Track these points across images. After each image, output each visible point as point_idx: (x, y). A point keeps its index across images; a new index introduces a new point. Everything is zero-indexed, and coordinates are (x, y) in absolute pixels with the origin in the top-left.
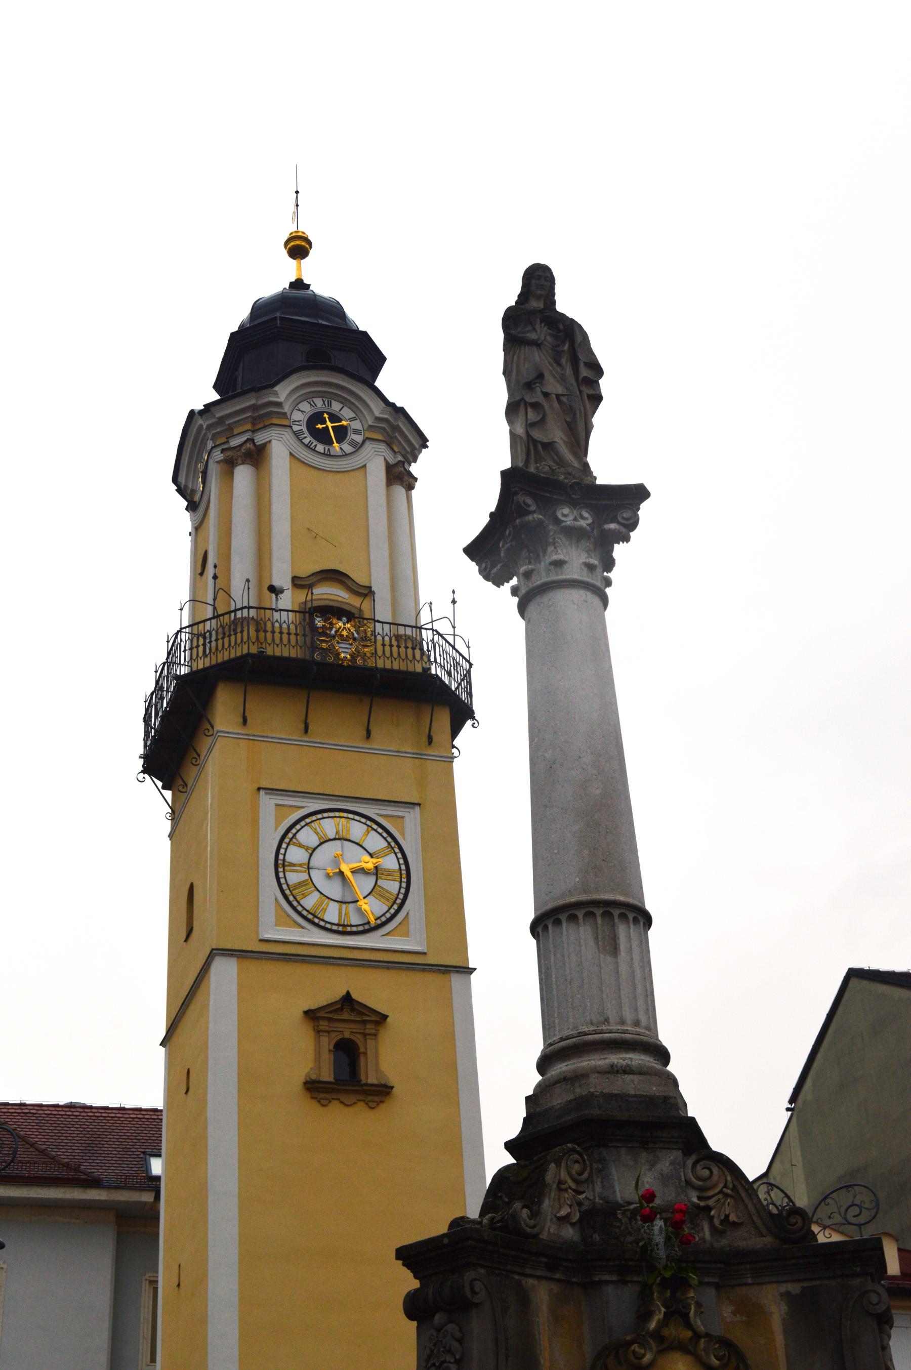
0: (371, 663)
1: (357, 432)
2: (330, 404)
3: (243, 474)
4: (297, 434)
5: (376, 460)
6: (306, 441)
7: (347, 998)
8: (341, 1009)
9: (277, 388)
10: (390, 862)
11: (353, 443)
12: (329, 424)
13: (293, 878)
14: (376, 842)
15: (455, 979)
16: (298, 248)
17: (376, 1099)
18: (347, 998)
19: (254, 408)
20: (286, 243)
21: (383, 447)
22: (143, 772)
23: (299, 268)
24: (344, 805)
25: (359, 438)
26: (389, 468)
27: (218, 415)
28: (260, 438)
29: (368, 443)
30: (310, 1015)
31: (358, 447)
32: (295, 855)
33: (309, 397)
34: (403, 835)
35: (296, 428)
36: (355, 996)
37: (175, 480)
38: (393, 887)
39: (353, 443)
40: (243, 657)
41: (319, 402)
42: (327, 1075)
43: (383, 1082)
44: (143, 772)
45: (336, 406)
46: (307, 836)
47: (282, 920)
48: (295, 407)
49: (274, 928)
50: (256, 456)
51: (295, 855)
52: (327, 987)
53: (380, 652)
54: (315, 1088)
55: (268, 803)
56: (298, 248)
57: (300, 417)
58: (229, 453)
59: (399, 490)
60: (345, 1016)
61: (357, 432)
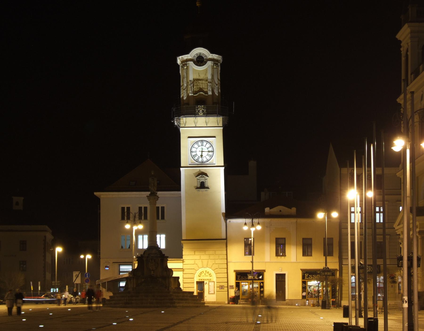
13: (193, 154)
32: (194, 150)
42: (199, 186)
51: (194, 150)
54: (197, 188)
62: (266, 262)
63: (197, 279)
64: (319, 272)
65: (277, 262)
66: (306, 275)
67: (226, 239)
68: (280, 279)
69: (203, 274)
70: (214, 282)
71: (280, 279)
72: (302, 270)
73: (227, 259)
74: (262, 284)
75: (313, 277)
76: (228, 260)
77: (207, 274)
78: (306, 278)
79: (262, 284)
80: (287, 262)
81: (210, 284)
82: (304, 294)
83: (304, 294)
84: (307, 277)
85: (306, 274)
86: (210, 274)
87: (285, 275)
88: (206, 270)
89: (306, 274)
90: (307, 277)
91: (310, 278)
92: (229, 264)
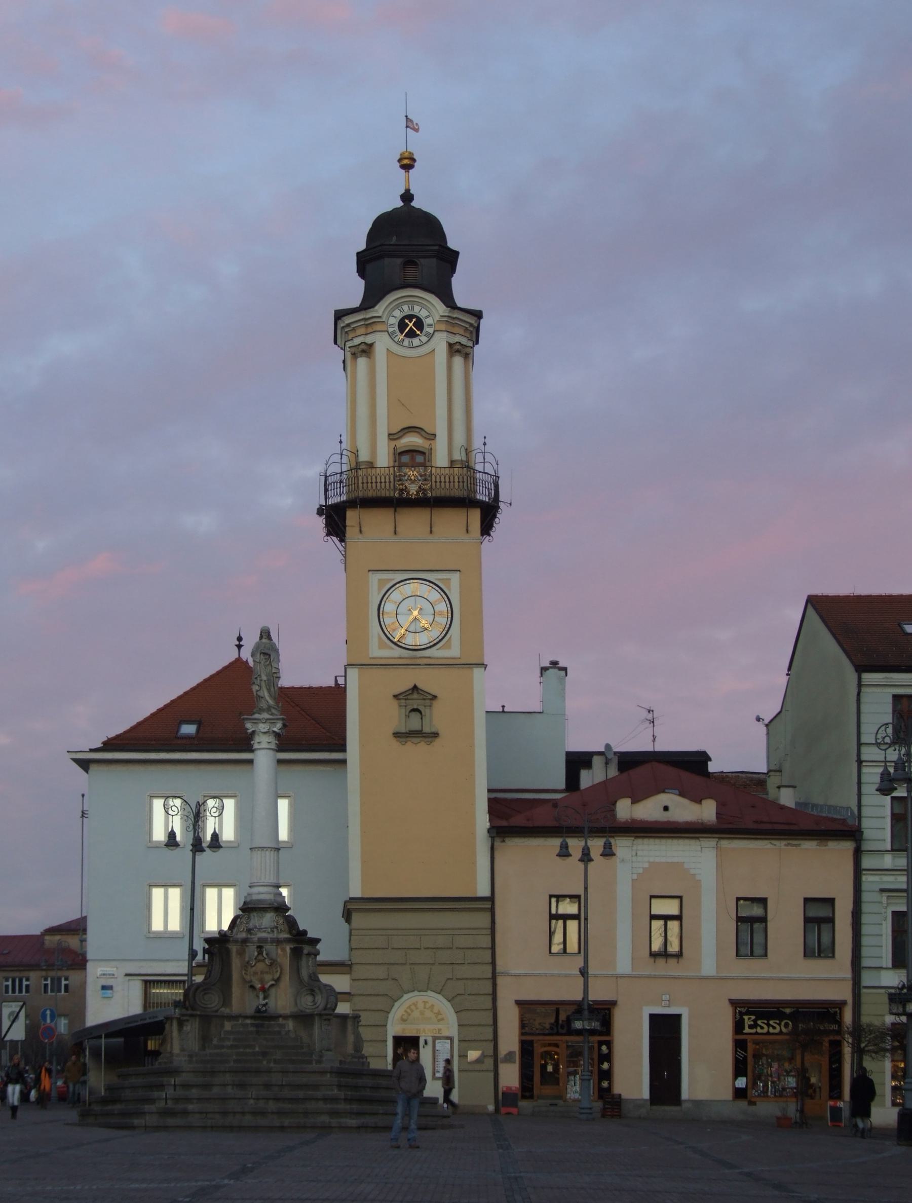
0: (429, 495)
1: (430, 326)
2: (413, 309)
3: (362, 361)
4: (391, 335)
5: (440, 344)
6: (396, 339)
7: (415, 688)
8: (412, 693)
9: (377, 308)
10: (442, 607)
11: (427, 335)
12: (411, 325)
14: (435, 595)
15: (477, 671)
16: (407, 163)
17: (430, 740)
18: (415, 688)
19: (365, 319)
20: (399, 161)
21: (445, 334)
22: (328, 535)
23: (408, 181)
24: (416, 574)
25: (431, 330)
26: (450, 345)
27: (347, 322)
28: (369, 339)
29: (436, 333)
30: (395, 696)
31: (430, 337)
33: (398, 306)
34: (450, 590)
35: (390, 330)
36: (419, 686)
37: (335, 342)
38: (443, 621)
39: (427, 335)
40: (356, 498)
41: (405, 308)
43: (433, 730)
44: (328, 535)
45: (417, 309)
46: (396, 596)
47: (382, 646)
48: (390, 315)
49: (377, 651)
50: (367, 350)
52: (404, 680)
53: (434, 487)
55: (374, 578)
56: (407, 163)
57: (394, 321)
58: (353, 350)
59: (458, 361)
60: (415, 696)
61: (430, 326)
62: (618, 977)
63: (394, 1028)
64: (788, 1011)
65: (655, 977)
66: (748, 1020)
67: (491, 899)
68: (665, 1032)
69: (416, 1014)
70: (451, 1039)
71: (665, 1032)
72: (734, 1003)
73: (493, 963)
74: (604, 1048)
75: (768, 1025)
76: (499, 969)
77: (428, 1014)
78: (747, 1030)
79: (604, 1048)
80: (687, 978)
81: (439, 1045)
82: (741, 1082)
83: (741, 1082)
84: (750, 1027)
85: (746, 1018)
86: (439, 1013)
87: (678, 1017)
88: (425, 999)
89: (746, 1018)
90: (750, 1027)
91: (759, 1030)
92: (500, 981)
